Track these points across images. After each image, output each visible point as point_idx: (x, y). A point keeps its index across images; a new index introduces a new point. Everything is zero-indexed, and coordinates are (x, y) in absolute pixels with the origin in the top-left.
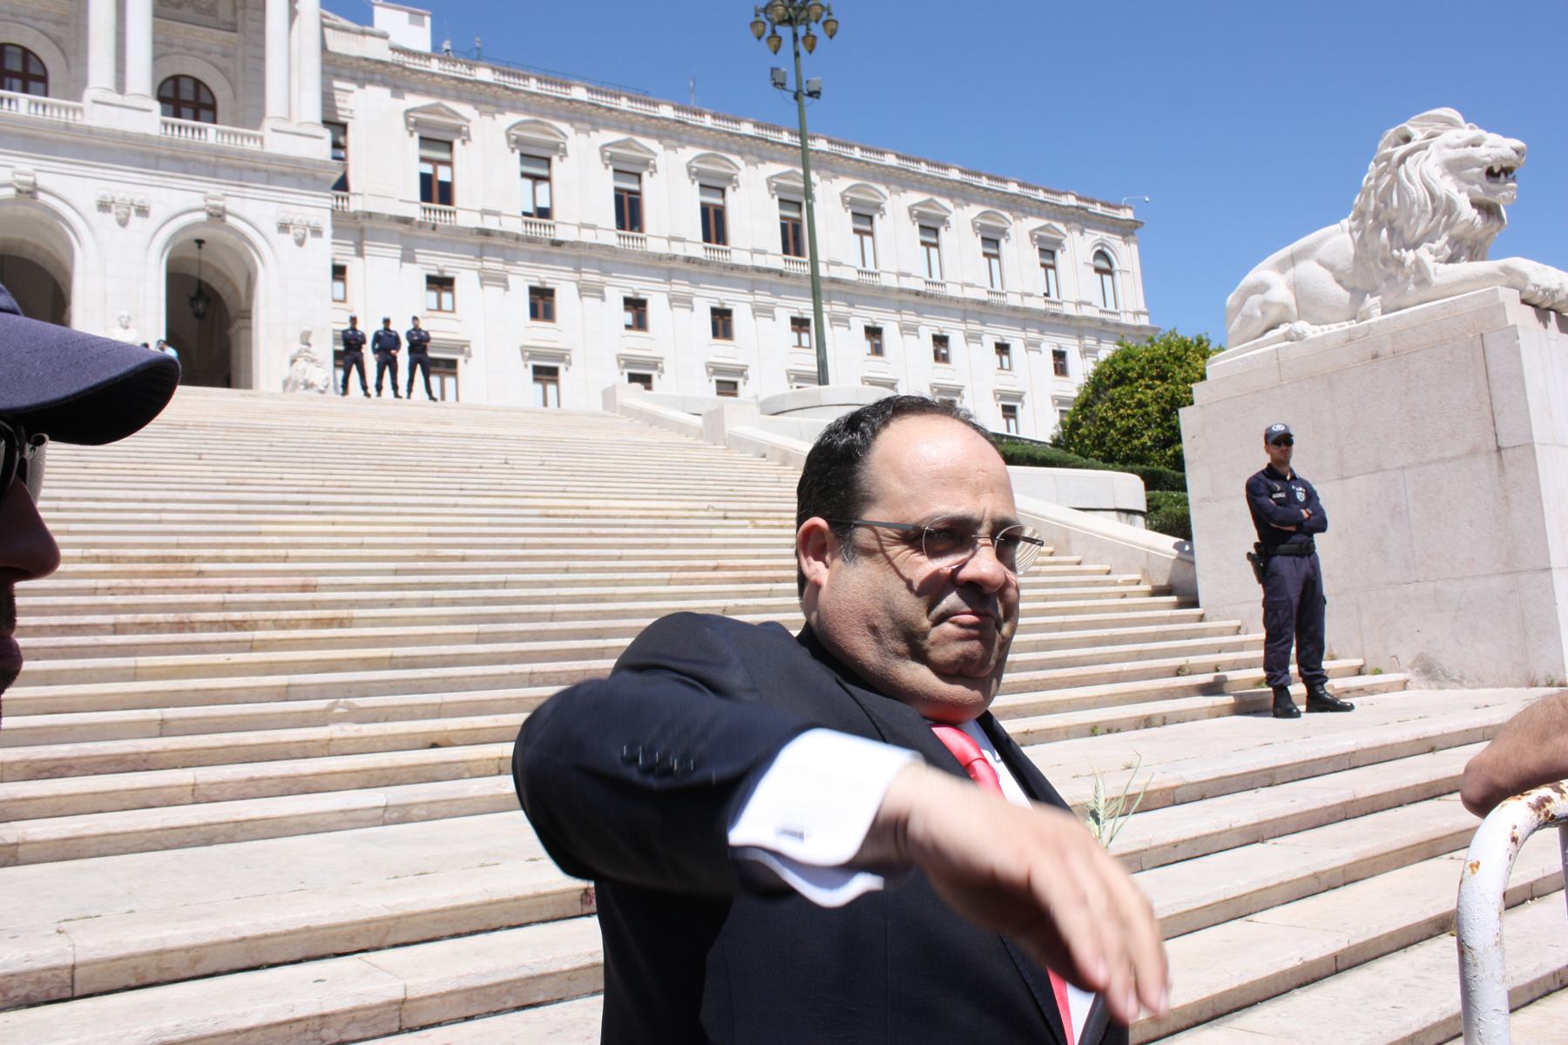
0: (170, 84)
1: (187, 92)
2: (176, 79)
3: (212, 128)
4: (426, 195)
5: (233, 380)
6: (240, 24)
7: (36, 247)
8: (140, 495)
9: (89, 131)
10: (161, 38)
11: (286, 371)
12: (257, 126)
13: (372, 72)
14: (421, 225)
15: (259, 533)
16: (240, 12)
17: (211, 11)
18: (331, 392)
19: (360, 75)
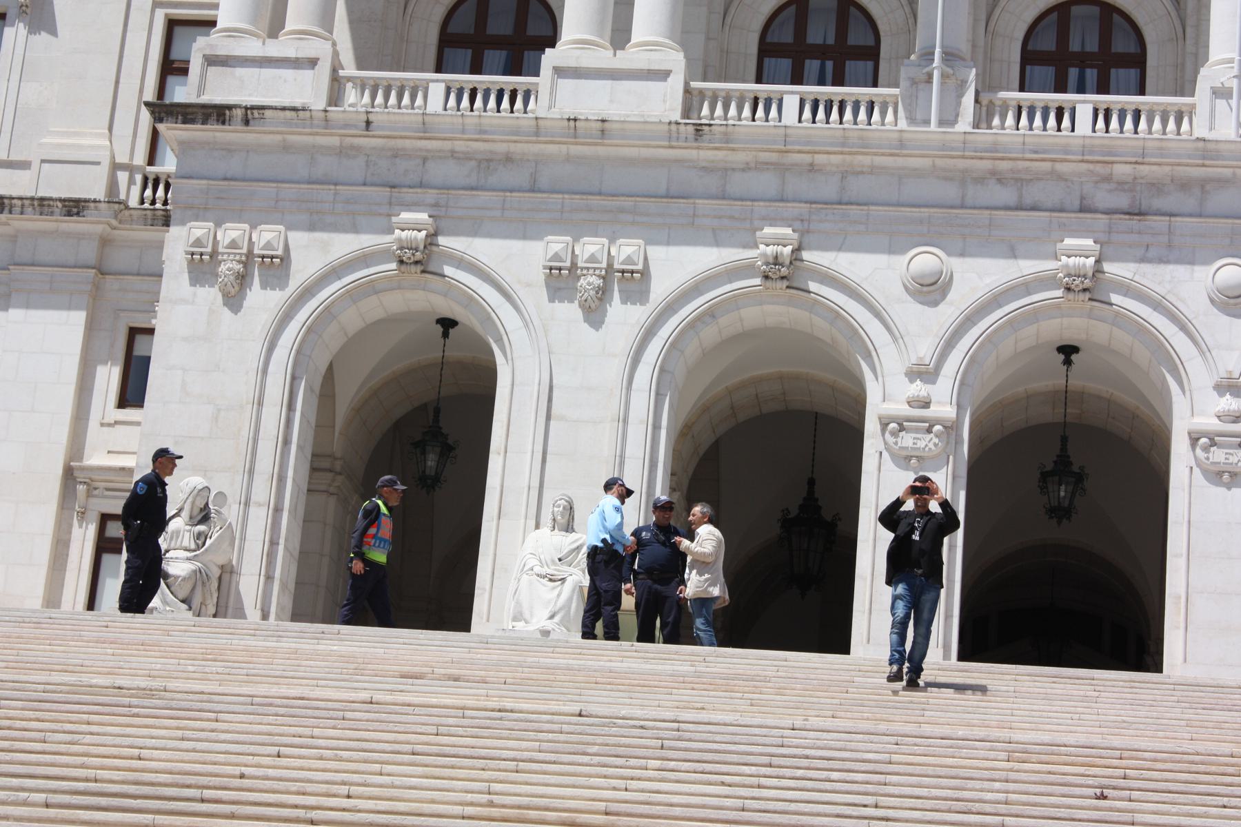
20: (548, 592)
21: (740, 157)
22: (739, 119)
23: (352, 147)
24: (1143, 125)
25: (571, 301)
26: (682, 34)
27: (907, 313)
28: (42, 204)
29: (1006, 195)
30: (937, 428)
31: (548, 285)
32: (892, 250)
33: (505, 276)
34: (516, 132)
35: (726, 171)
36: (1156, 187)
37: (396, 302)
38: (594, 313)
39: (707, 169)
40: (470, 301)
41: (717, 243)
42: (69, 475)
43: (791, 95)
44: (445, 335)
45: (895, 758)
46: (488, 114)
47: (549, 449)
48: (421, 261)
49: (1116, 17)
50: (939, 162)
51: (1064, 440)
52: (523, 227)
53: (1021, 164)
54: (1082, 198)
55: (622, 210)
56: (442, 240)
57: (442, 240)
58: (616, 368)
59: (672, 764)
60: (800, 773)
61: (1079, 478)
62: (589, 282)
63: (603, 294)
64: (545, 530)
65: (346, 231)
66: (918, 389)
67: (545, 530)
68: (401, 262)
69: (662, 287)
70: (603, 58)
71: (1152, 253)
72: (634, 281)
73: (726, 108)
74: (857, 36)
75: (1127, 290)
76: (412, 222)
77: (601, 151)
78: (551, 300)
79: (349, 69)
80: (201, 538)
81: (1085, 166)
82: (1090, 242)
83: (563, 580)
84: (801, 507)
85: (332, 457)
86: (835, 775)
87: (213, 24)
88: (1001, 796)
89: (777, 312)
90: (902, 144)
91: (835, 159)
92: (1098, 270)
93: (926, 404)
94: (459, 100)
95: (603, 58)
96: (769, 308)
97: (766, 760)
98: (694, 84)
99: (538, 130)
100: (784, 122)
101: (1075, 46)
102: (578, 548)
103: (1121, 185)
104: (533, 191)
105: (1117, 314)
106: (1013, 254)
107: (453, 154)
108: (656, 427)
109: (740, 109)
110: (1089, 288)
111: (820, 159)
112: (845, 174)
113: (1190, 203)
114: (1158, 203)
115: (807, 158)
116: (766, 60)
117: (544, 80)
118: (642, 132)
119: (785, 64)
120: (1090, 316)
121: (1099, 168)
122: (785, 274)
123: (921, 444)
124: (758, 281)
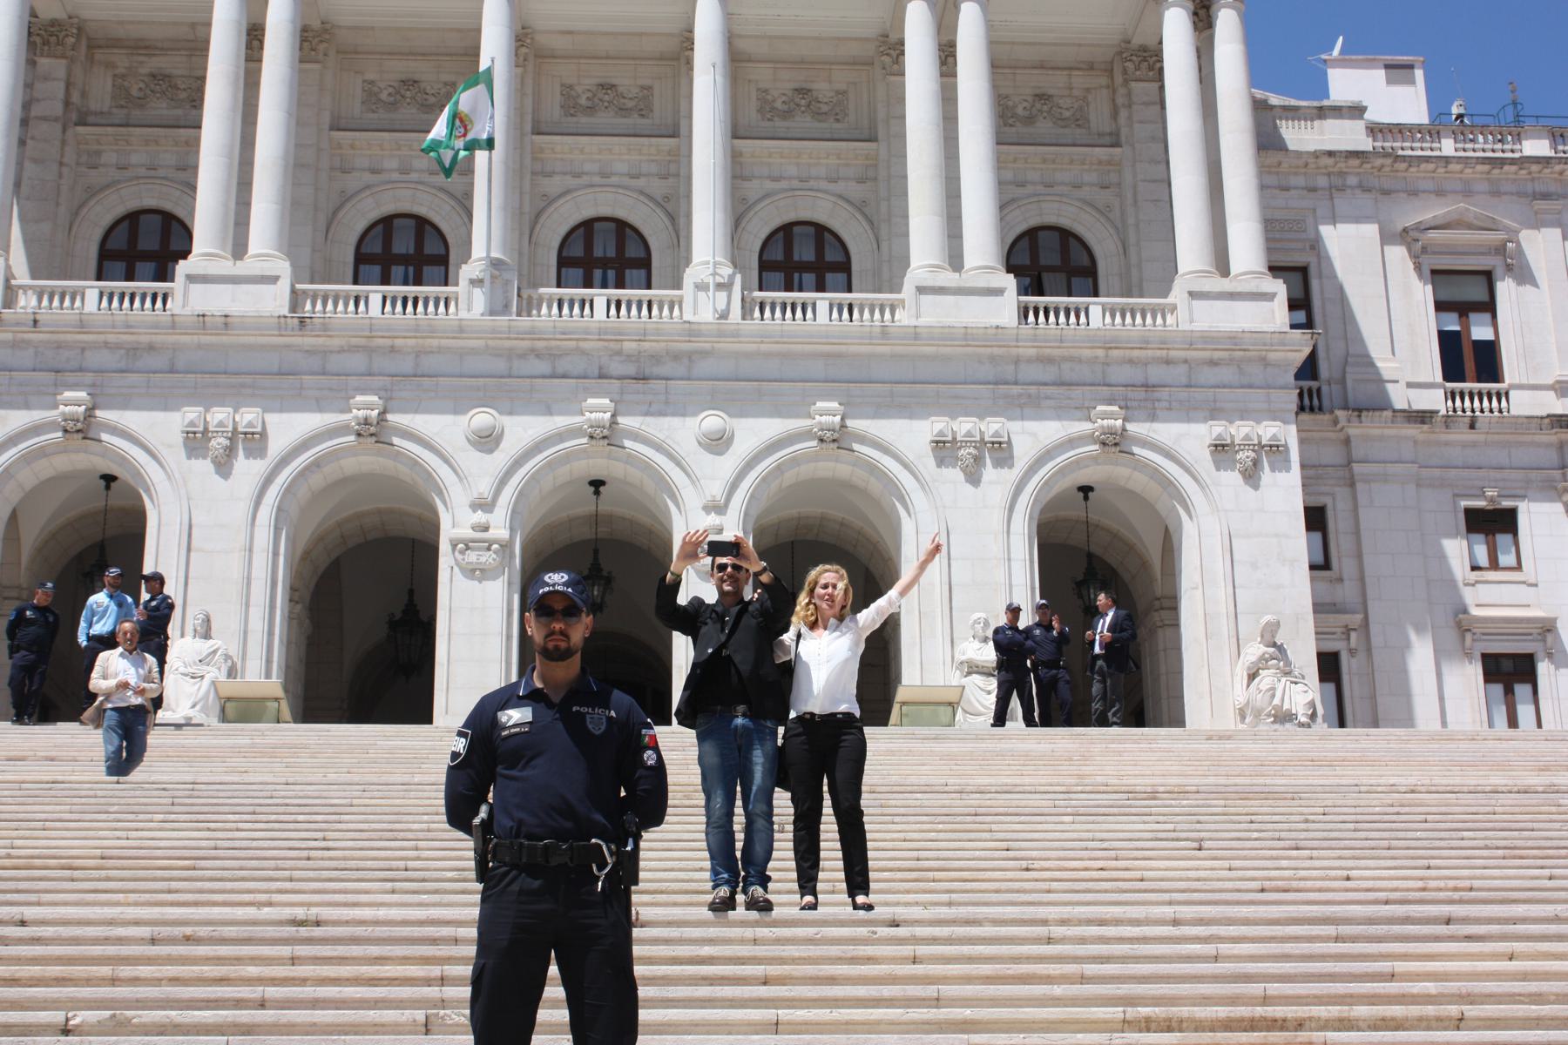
0: (1025, 243)
1: (1049, 257)
2: (1031, 234)
3: (1096, 308)
4: (1452, 368)
5: (1149, 714)
6: (1124, 131)
7: (842, 524)
8: (1168, 911)
9: (915, 334)
10: (1009, 175)
11: (1239, 692)
12: (1166, 297)
13: (1342, 174)
14: (1448, 421)
15: (1392, 977)
16: (1123, 114)
17: (1080, 120)
18: (1320, 727)
19: (1322, 182)
21: (336, 343)
22: (343, 313)
23: (23, 341)
24: (655, 311)
25: (205, 458)
26: (289, 245)
27: (471, 459)
29: (543, 367)
30: (495, 546)
31: (185, 445)
32: (457, 411)
33: (150, 440)
34: (156, 326)
35: (325, 353)
36: (656, 358)
37: (62, 463)
38: (223, 466)
39: (311, 352)
40: (123, 460)
41: (320, 410)
43: (375, 293)
44: (108, 487)
45: (355, 801)
46: (142, 313)
47: (191, 574)
48: (82, 429)
49: (628, 230)
50: (490, 342)
51: (596, 552)
52: (165, 401)
53: (553, 343)
54: (600, 368)
55: (243, 386)
56: (98, 413)
57: (98, 413)
58: (242, 509)
59: (173, 817)
60: (273, 817)
61: (608, 581)
62: (219, 442)
63: (230, 451)
64: (188, 638)
65: (19, 408)
66: (480, 517)
67: (188, 638)
68: (66, 431)
70: (227, 267)
71: (654, 408)
72: (255, 441)
73: (325, 304)
74: (431, 247)
75: (636, 437)
76: (74, 400)
77: (224, 338)
78: (189, 458)
79: (22, 277)
81: (601, 344)
82: (607, 401)
83: (202, 677)
84: (404, 612)
85: (19, 587)
86: (301, 818)
88: (424, 826)
89: (368, 461)
90: (461, 330)
91: (411, 342)
92: (613, 422)
93: (486, 529)
94: (110, 302)
95: (227, 267)
96: (362, 458)
97: (250, 809)
98: (298, 286)
99: (174, 324)
100: (371, 314)
101: (598, 252)
102: (215, 652)
103: (629, 358)
104: (172, 371)
105: (629, 455)
106: (549, 411)
107: (106, 345)
108: (276, 554)
109: (346, 305)
110: (608, 436)
111: (398, 342)
112: (419, 353)
113: (680, 370)
114: (657, 371)
115: (388, 342)
116: (362, 267)
117: (177, 285)
118: (256, 324)
119: (377, 269)
120: (609, 457)
121: (612, 345)
122: (374, 432)
123: (483, 559)
124: (352, 438)
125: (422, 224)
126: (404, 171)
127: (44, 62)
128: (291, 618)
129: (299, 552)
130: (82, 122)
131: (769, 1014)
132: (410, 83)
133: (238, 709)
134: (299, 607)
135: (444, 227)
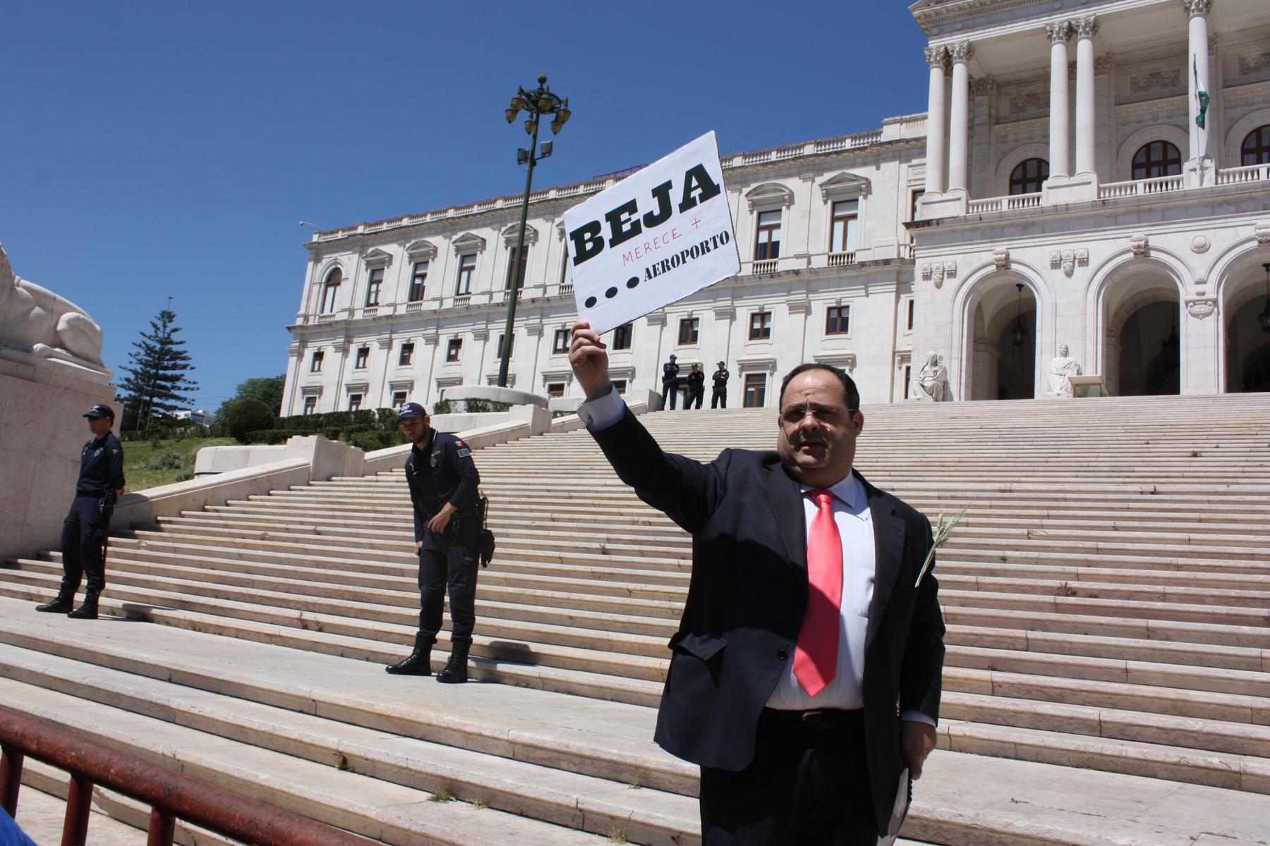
20: (1059, 380)
21: (1122, 210)
26: (1098, 166)
28: (876, 263)
34: (1035, 213)
37: (998, 281)
40: (1024, 277)
42: (894, 353)
43: (1140, 184)
46: (1029, 207)
48: (1004, 265)
62: (1067, 265)
66: (1200, 288)
69: (1094, 263)
70: (1066, 181)
74: (1171, 155)
80: (936, 372)
87: (923, 191)
89: (1142, 267)
93: (1203, 294)
95: (1066, 181)
99: (1043, 211)
107: (1013, 225)
118: (1082, 206)
122: (1143, 252)
125: (1165, 144)
126: (1155, 119)
127: (978, 99)
128: (1107, 345)
129: (1112, 314)
130: (997, 123)
131: (1185, 536)
132: (1155, 75)
133: (1081, 389)
134: (1113, 340)
135: (1177, 144)
